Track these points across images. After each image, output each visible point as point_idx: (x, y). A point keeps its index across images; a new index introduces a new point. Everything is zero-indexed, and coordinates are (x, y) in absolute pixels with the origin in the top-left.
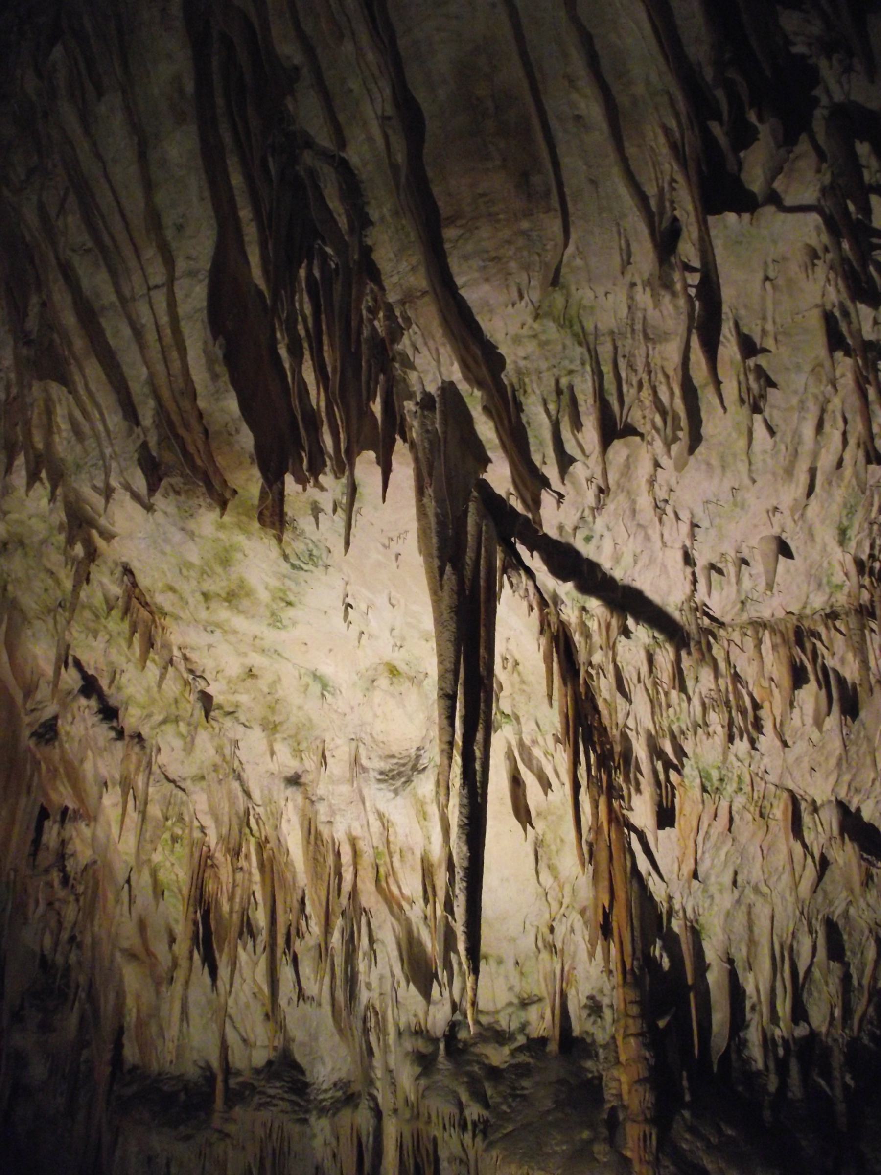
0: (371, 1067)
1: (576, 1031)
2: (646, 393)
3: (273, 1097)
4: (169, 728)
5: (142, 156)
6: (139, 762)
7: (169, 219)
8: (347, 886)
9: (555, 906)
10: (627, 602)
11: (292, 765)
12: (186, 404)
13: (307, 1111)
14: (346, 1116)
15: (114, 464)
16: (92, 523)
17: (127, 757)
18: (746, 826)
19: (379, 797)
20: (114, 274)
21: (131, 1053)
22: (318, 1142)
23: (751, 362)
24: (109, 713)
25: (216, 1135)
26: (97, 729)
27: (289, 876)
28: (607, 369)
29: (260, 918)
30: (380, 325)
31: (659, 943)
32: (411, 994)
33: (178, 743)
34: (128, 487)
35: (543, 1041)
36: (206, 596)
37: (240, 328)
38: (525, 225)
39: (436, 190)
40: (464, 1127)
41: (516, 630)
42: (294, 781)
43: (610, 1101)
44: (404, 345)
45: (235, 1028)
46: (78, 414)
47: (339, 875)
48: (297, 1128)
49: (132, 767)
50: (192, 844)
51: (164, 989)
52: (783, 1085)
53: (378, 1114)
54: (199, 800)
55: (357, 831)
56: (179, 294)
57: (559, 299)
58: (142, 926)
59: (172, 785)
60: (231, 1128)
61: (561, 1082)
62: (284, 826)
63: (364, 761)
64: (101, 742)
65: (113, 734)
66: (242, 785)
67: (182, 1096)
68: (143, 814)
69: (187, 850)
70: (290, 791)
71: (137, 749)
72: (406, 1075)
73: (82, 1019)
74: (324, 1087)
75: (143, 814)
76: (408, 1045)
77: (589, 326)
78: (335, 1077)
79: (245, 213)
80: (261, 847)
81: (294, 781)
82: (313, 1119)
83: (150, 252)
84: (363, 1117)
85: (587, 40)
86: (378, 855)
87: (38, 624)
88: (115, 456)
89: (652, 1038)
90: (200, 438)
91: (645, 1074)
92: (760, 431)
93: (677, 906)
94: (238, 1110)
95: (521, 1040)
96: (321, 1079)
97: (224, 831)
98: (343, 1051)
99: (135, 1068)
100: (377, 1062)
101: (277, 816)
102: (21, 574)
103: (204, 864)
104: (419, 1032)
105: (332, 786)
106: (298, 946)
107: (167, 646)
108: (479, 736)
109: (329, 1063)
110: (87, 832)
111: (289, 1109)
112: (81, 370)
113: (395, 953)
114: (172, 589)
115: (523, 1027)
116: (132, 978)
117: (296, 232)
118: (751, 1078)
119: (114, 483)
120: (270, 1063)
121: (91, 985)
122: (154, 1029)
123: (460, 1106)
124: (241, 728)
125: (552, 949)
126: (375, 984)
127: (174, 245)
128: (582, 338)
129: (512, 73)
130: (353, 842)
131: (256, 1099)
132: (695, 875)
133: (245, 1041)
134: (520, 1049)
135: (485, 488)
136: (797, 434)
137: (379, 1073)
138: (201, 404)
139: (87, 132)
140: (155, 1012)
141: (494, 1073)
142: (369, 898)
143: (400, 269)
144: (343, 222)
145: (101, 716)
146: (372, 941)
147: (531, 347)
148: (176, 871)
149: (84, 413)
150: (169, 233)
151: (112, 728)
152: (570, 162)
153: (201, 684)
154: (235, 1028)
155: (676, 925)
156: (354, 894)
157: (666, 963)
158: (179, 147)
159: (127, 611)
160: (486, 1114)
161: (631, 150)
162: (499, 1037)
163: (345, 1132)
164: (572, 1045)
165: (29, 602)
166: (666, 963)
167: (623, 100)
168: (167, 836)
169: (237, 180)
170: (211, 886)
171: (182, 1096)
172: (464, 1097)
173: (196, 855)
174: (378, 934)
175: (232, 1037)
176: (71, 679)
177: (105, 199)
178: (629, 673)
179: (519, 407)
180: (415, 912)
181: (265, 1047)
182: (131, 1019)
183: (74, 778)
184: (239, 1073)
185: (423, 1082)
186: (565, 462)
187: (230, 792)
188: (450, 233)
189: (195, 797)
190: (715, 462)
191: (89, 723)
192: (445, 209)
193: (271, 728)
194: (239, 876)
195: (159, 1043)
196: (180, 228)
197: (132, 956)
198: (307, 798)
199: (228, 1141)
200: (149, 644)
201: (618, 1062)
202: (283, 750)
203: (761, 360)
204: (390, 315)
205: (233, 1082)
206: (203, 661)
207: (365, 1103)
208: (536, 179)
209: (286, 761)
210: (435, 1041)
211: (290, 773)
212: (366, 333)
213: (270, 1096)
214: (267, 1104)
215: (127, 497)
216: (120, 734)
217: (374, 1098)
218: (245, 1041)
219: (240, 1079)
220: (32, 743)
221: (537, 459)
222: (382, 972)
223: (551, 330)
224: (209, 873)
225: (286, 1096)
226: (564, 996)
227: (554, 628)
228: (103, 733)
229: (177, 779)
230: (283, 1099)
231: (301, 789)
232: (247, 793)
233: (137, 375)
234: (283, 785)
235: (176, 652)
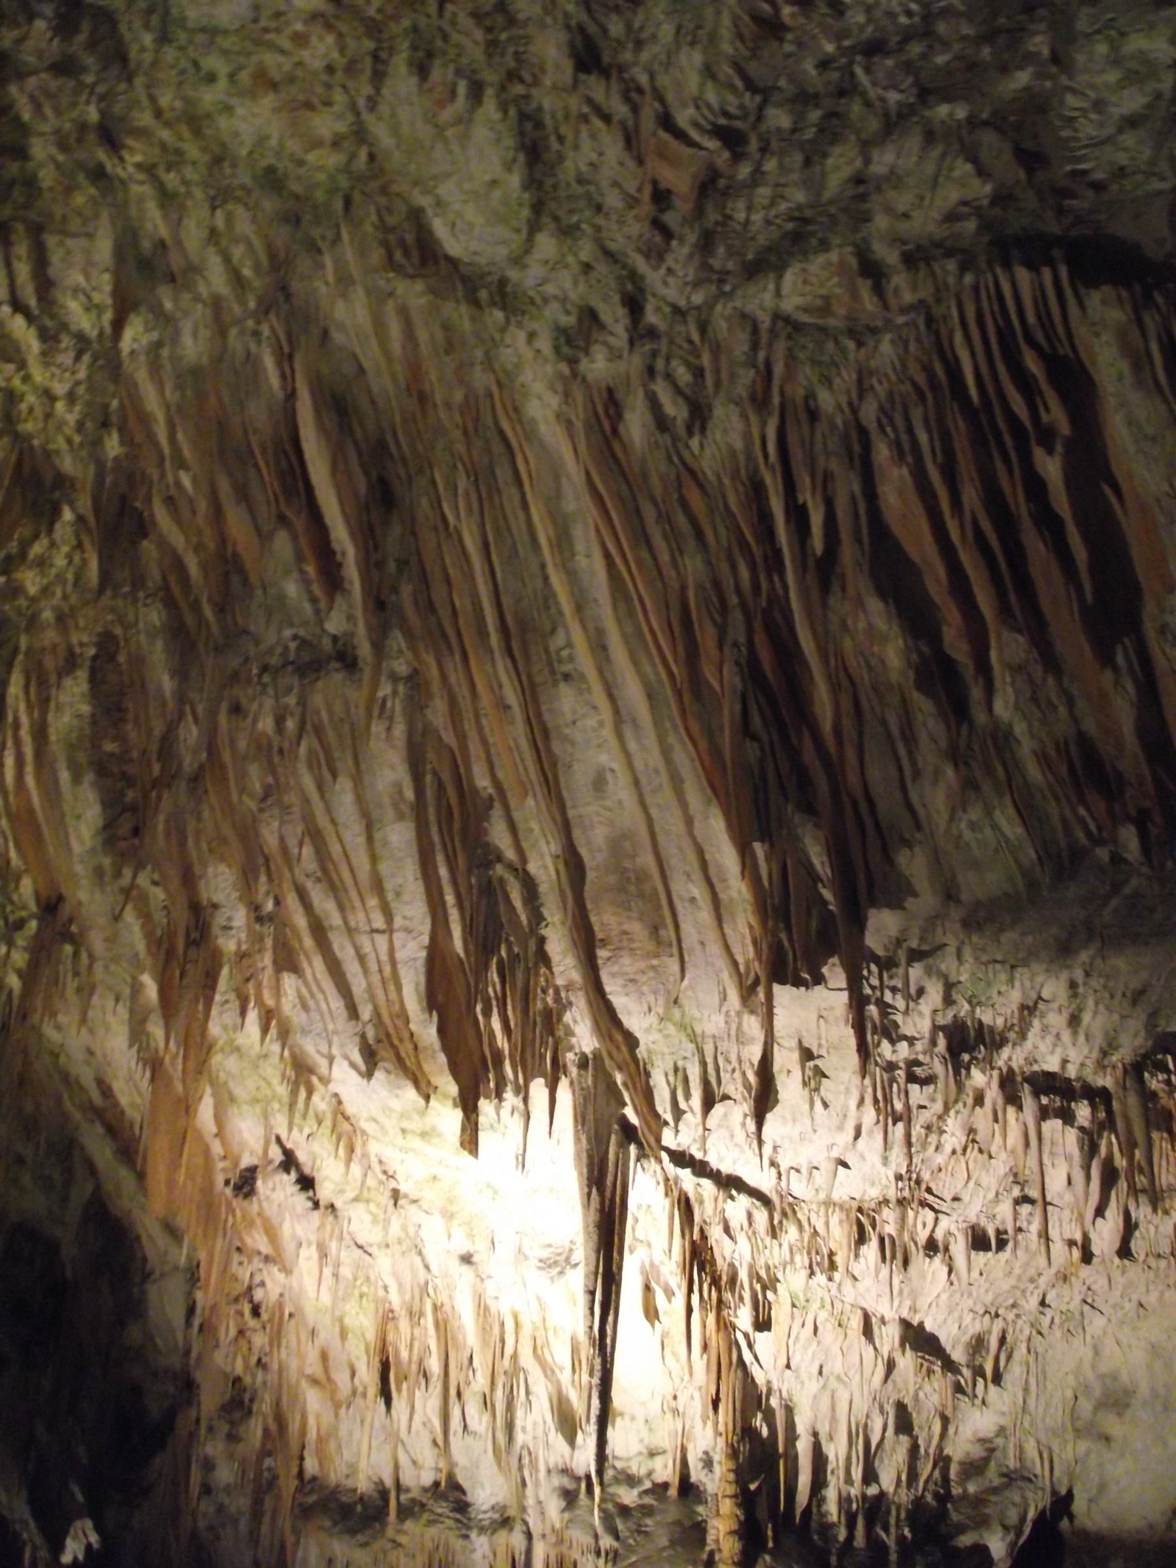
0: (524, 1496)
1: (693, 1479)
2: (737, 1075)
4: (361, 1207)
5: (370, 839)
7: (389, 886)
8: (509, 1350)
9: (677, 1381)
10: (730, 1184)
11: (464, 1247)
12: (399, 1023)
13: (469, 1528)
14: (502, 1536)
15: (335, 1039)
16: (311, 1071)
17: (322, 1227)
18: (828, 1332)
19: (539, 1281)
20: (341, 908)
21: (311, 1466)
22: (477, 1556)
23: (811, 1064)
24: (306, 1183)
28: (709, 1060)
29: (434, 1365)
30: (550, 1000)
31: (759, 1416)
32: (559, 1442)
33: (368, 1218)
34: (346, 1057)
35: (665, 1486)
36: (404, 1131)
37: (446, 990)
38: (655, 962)
39: (593, 919)
40: (598, 1553)
41: (646, 1193)
42: (467, 1259)
43: (710, 1546)
44: (568, 1017)
46: (304, 991)
47: (503, 1341)
48: (458, 1544)
50: (376, 1301)
51: (343, 1411)
52: (851, 1537)
53: (529, 1536)
54: (383, 1264)
55: (518, 1308)
56: (397, 943)
57: (676, 1013)
58: (324, 1357)
60: (402, 1539)
61: (678, 1523)
63: (526, 1250)
65: (310, 1204)
67: (359, 1508)
68: (336, 1275)
69: (372, 1306)
70: (465, 1268)
72: (554, 1506)
73: (266, 1431)
75: (336, 1275)
76: (557, 1481)
77: (698, 1031)
78: (493, 1501)
79: (450, 899)
80: (435, 1308)
81: (467, 1259)
82: (473, 1535)
83: (373, 902)
84: (517, 1540)
85: (700, 852)
86: (535, 1329)
87: (245, 1107)
88: (335, 1032)
89: (745, 1499)
90: (410, 1046)
91: (735, 1527)
92: (818, 1105)
93: (775, 1387)
94: (409, 1525)
95: (648, 1485)
97: (408, 1297)
98: (500, 1479)
99: (314, 1479)
100: (530, 1491)
101: (451, 1287)
102: (234, 1070)
103: (387, 1318)
104: (565, 1471)
105: (498, 1266)
106: (466, 1395)
107: (365, 1155)
108: (611, 1318)
109: (487, 1490)
110: (281, 1277)
112: (310, 963)
113: (547, 1406)
114: (375, 1120)
115: (650, 1474)
116: (313, 1401)
117: (487, 930)
118: (826, 1529)
119: (335, 1051)
120: (437, 1484)
121: (278, 1403)
122: (332, 1445)
123: (596, 1537)
125: (675, 1412)
126: (529, 1427)
127: (393, 905)
128: (693, 1038)
129: (647, 860)
130: (516, 1317)
131: (426, 1516)
132: (788, 1366)
133: (414, 1462)
134: (646, 1492)
135: (624, 1117)
136: (846, 1107)
137: (530, 1501)
138: (413, 1026)
139: (322, 797)
140: (333, 1432)
141: (624, 1510)
142: (527, 1359)
143: (565, 965)
144: (524, 918)
146: (528, 1393)
147: (656, 1036)
148: (363, 1322)
149: (313, 996)
150: (390, 896)
152: (686, 927)
153: (393, 1184)
155: (774, 1402)
156: (515, 1356)
157: (765, 1432)
158: (399, 836)
159: (334, 1126)
160: (616, 1544)
161: (728, 930)
162: (631, 1480)
163: (501, 1551)
164: (688, 1489)
165: (239, 1092)
166: (765, 1432)
167: (723, 896)
168: (357, 1293)
169: (443, 872)
170: (391, 1337)
171: (359, 1508)
172: (600, 1530)
174: (532, 1388)
175: (403, 1459)
176: (276, 1154)
177: (335, 849)
178: (734, 1224)
179: (648, 1075)
180: (565, 1377)
182: (312, 1435)
183: (272, 1233)
184: (408, 1490)
185: (567, 1515)
186: (678, 1113)
187: (412, 1266)
188: (602, 954)
190: (788, 1116)
192: (599, 935)
193: (449, 1216)
194: (417, 1331)
196: (398, 894)
197: (315, 1382)
200: (351, 1150)
201: (718, 1514)
202: (459, 1233)
203: (818, 1062)
204: (558, 999)
205: (403, 1498)
206: (393, 1166)
207: (518, 1527)
208: (662, 933)
210: (578, 1479)
211: (463, 1251)
212: (539, 1005)
215: (346, 1064)
216: (316, 1205)
217: (526, 1523)
218: (414, 1462)
220: (229, 1191)
221: (659, 1109)
222: (535, 1422)
223: (671, 1029)
224: (390, 1325)
226: (684, 1450)
227: (676, 1194)
228: (301, 1201)
232: (427, 1267)
233: (358, 985)
234: (457, 1262)
235: (374, 1159)
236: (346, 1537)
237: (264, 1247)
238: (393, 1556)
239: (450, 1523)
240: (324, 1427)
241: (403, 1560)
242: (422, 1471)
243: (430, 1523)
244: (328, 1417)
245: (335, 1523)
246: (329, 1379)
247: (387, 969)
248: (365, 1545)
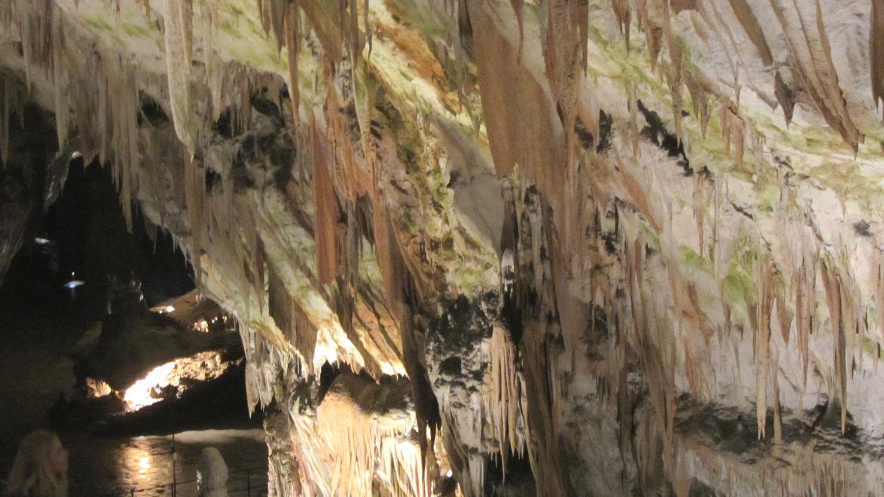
3: (831, 442)
6: (710, 195)
15: (741, 71)
25: (778, 463)
26: (664, 164)
27: (856, 300)
45: (786, 378)
49: (704, 201)
59: (741, 215)
62: (852, 263)
64: (669, 174)
65: (681, 170)
66: (815, 230)
67: (740, 427)
70: (860, 239)
71: (706, 183)
74: (874, 435)
81: (862, 229)
82: (865, 459)
94: (795, 446)
96: (870, 428)
111: (844, 451)
122: (704, 368)
124: (816, 191)
133: (795, 388)
140: (705, 356)
145: (667, 152)
151: (680, 164)
154: (786, 378)
171: (740, 427)
173: (765, 269)
181: (814, 394)
184: (790, 412)
189: (761, 222)
191: (656, 158)
195: (711, 381)
198: (876, 247)
199: (789, 467)
209: (855, 212)
213: (827, 441)
214: (825, 448)
216: (689, 172)
219: (792, 417)
225: (841, 441)
228: (671, 166)
229: (744, 206)
230: (839, 443)
231: (871, 239)
232: (819, 237)
234: (853, 232)
236: (730, 454)
237: (622, 194)
238: (783, 473)
239: (840, 448)
240: (693, 353)
241: (792, 476)
242: (805, 399)
243: (819, 449)
244: (697, 342)
245: (717, 441)
246: (698, 310)
247: (814, 31)
248: (752, 462)
